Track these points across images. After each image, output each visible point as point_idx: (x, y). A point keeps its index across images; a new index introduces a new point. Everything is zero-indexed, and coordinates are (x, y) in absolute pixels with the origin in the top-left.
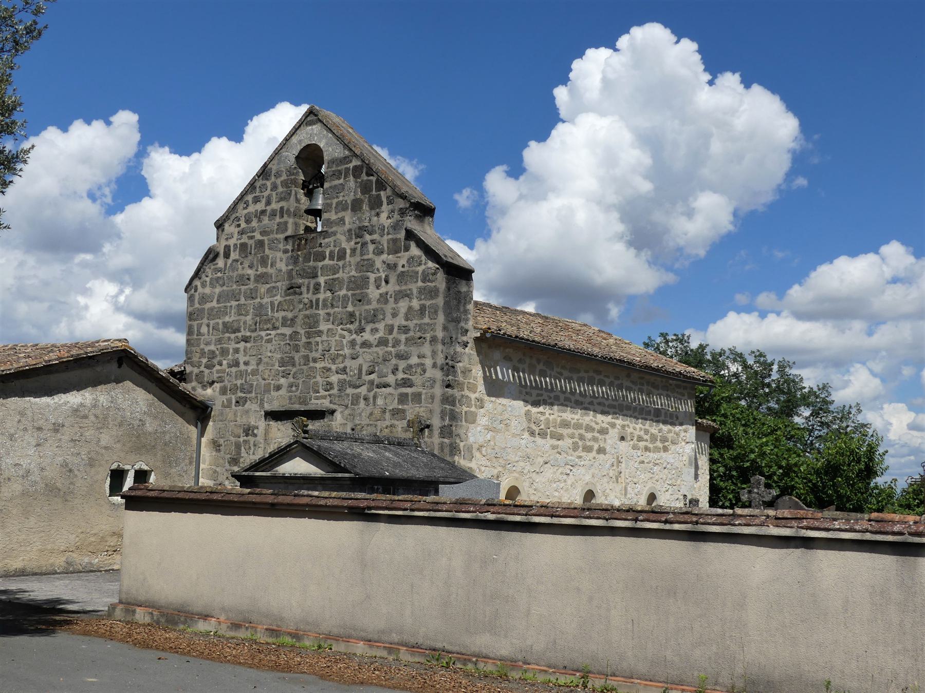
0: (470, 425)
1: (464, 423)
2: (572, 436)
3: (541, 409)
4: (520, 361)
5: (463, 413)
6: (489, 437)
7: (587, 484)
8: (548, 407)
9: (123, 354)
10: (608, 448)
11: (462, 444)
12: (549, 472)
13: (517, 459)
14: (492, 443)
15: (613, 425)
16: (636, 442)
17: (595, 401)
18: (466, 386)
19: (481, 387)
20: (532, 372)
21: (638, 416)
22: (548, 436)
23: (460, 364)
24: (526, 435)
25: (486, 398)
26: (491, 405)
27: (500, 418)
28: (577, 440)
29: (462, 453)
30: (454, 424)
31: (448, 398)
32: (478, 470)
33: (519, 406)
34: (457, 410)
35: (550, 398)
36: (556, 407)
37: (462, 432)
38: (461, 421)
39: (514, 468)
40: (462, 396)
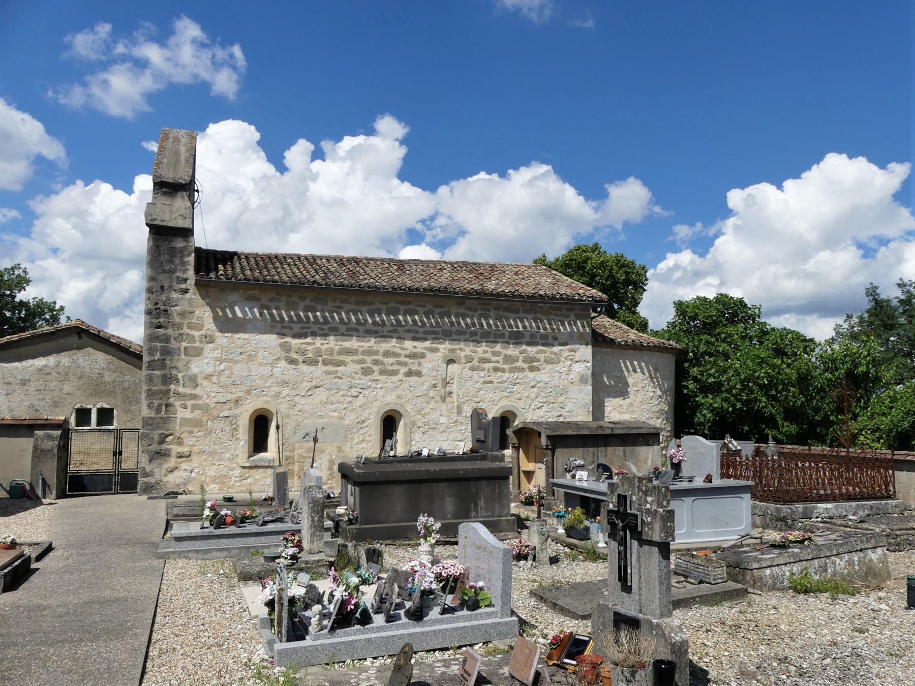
0: (192, 358)
1: (183, 356)
2: (361, 362)
3: (309, 340)
4: (271, 300)
5: (182, 348)
6: (222, 367)
7: (388, 404)
8: (318, 338)
9: (79, 330)
10: (424, 371)
11: (180, 376)
12: (321, 395)
13: (267, 384)
14: (227, 372)
15: (435, 350)
16: (477, 364)
17: (400, 329)
18: (185, 325)
19: (210, 325)
20: (290, 307)
21: (509, 341)
22: (320, 364)
23: (177, 308)
24: (283, 364)
25: (218, 334)
26: (225, 340)
27: (239, 350)
28: (371, 365)
29: (181, 382)
30: (168, 358)
31: (158, 337)
32: (205, 396)
33: (272, 340)
34: (172, 346)
35: (323, 329)
36: (332, 338)
37: (180, 365)
38: (179, 355)
39: (264, 393)
40: (181, 334)
